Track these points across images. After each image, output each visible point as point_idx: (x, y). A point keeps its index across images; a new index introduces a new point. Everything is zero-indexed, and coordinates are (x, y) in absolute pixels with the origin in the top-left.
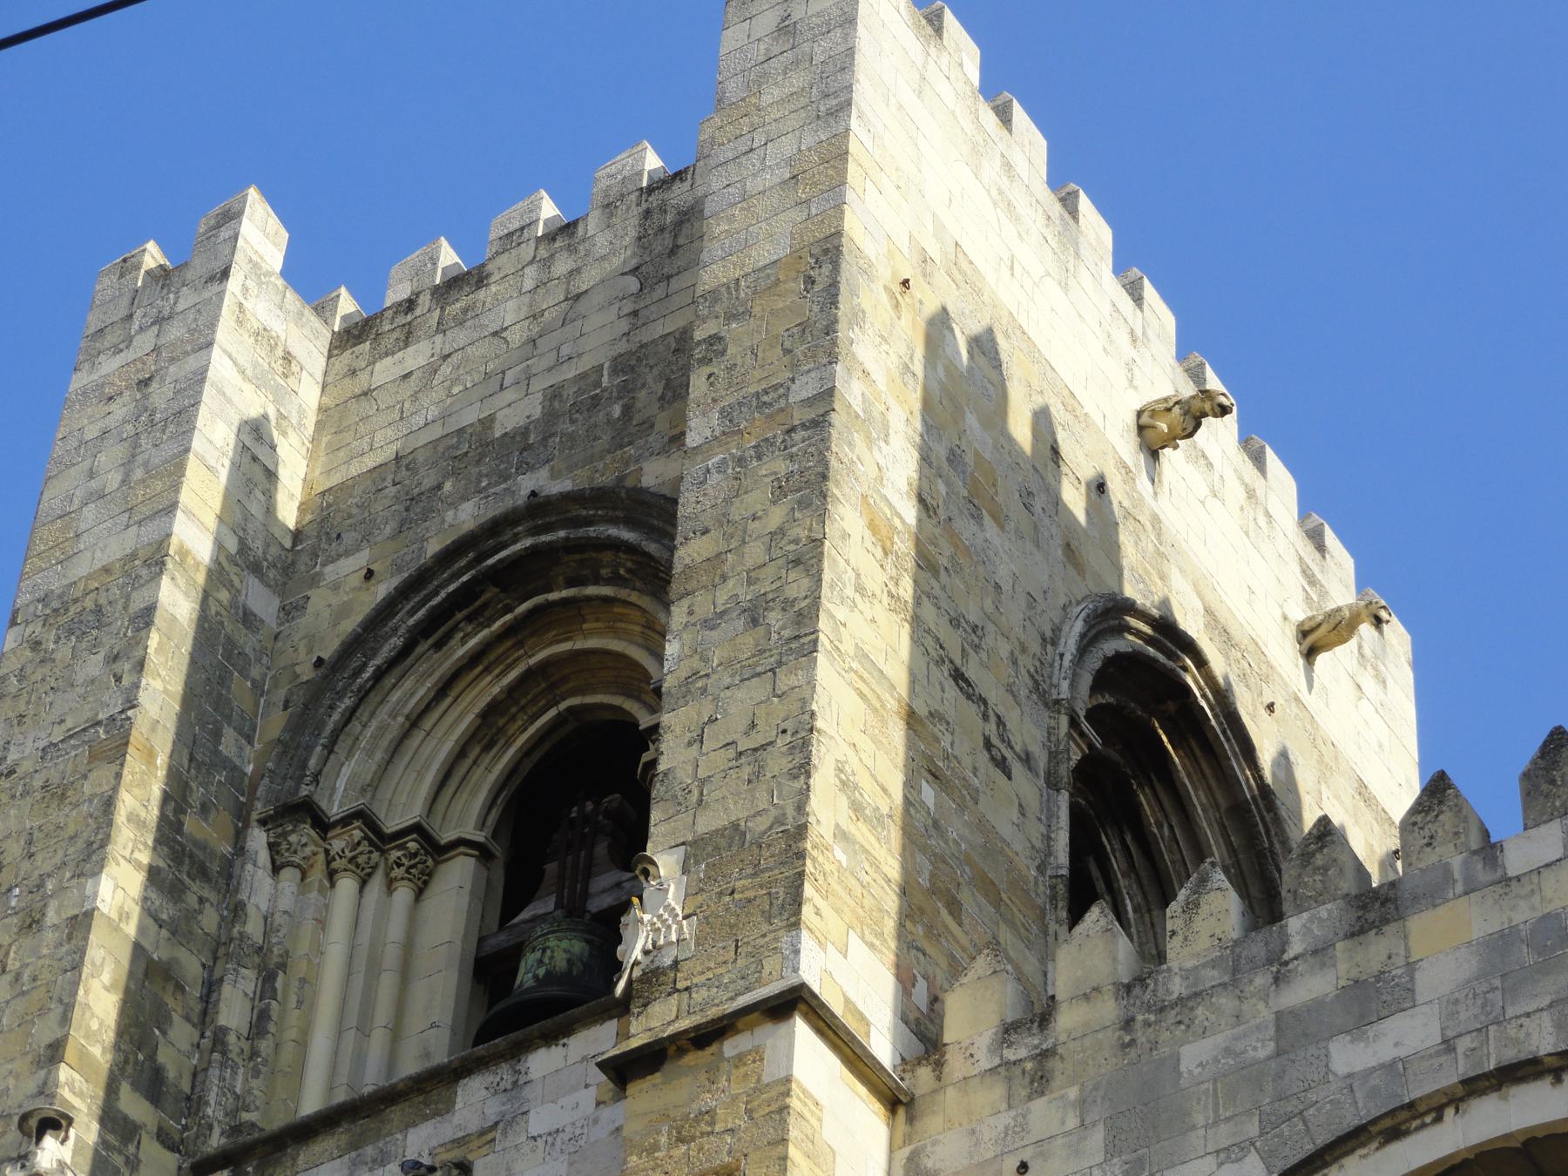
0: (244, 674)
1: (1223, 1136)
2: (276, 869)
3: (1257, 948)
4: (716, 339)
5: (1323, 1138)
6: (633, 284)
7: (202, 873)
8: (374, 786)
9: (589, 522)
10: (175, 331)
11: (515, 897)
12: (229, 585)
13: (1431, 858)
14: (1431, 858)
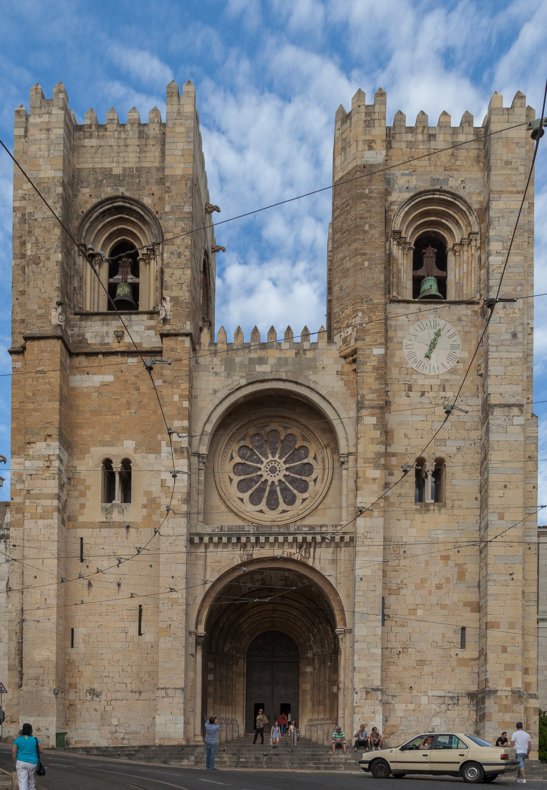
1: (241, 374)
9: (133, 205)
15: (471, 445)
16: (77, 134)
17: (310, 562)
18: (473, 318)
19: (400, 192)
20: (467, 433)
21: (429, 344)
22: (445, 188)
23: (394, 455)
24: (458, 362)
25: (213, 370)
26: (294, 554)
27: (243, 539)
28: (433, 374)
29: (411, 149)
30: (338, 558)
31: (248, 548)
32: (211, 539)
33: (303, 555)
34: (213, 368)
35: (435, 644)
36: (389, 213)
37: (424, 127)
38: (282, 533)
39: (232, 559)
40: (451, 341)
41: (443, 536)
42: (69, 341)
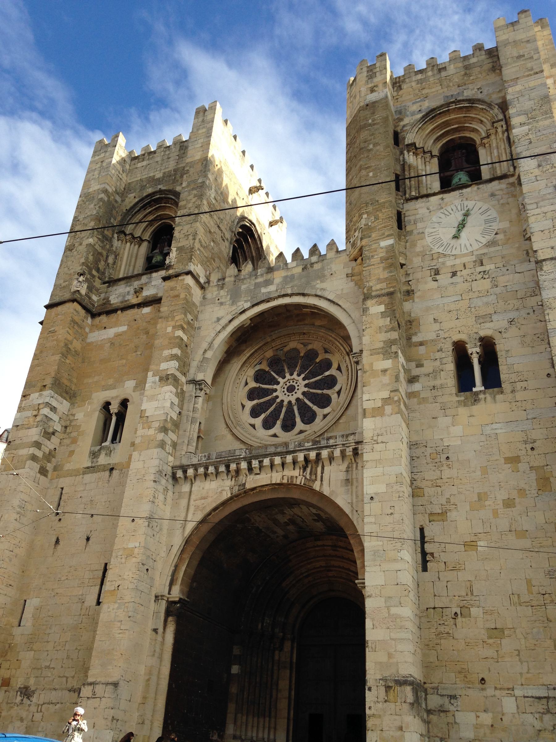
0: (115, 210)
2: (118, 240)
3: (254, 273)
4: (188, 170)
5: (259, 301)
6: (177, 157)
7: (107, 240)
8: (134, 229)
10: (107, 154)
11: (153, 249)
12: (113, 196)
13: (278, 264)
14: (278, 264)
15: (528, 314)
16: (133, 162)
17: (316, 486)
18: (510, 189)
19: (412, 115)
20: (521, 302)
21: (456, 225)
22: (460, 98)
23: (421, 344)
24: (496, 234)
25: (219, 301)
26: (297, 477)
27: (233, 466)
28: (466, 252)
29: (422, 84)
30: (354, 476)
31: (241, 477)
32: (196, 470)
33: (308, 477)
34: (219, 299)
35: (516, 599)
36: (402, 134)
37: (434, 66)
38: (279, 453)
39: (221, 492)
40: (484, 217)
41: (504, 431)
42: (94, 306)
